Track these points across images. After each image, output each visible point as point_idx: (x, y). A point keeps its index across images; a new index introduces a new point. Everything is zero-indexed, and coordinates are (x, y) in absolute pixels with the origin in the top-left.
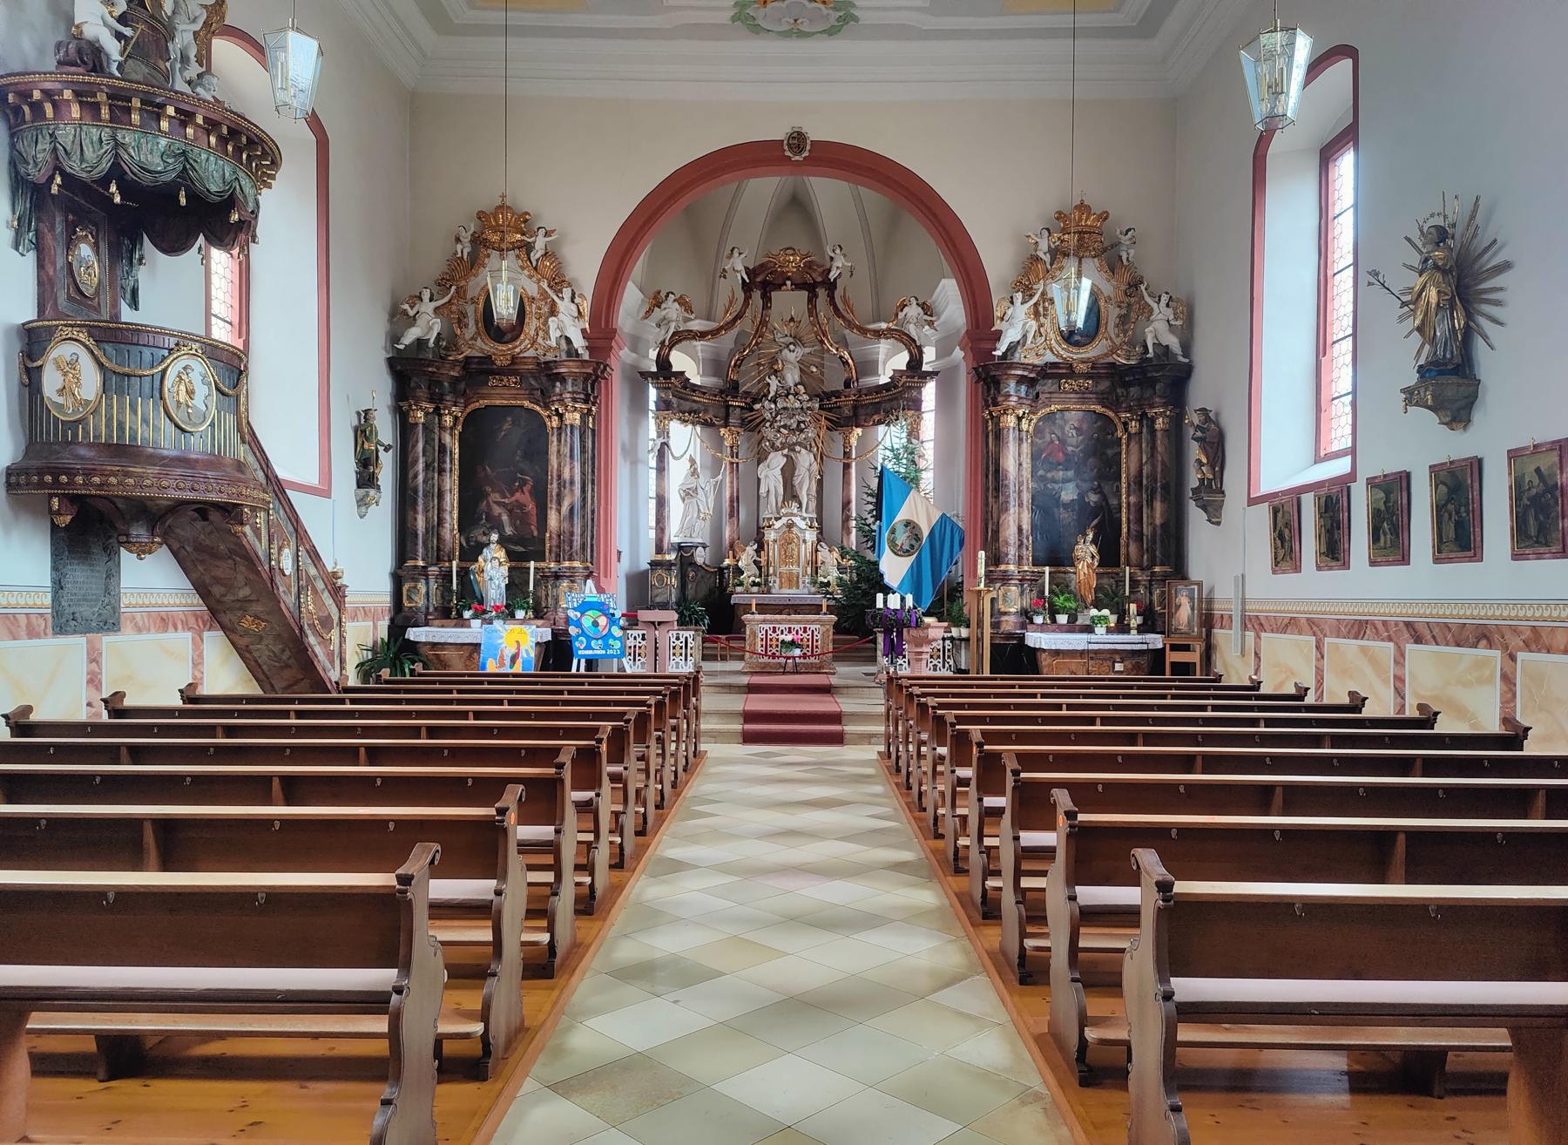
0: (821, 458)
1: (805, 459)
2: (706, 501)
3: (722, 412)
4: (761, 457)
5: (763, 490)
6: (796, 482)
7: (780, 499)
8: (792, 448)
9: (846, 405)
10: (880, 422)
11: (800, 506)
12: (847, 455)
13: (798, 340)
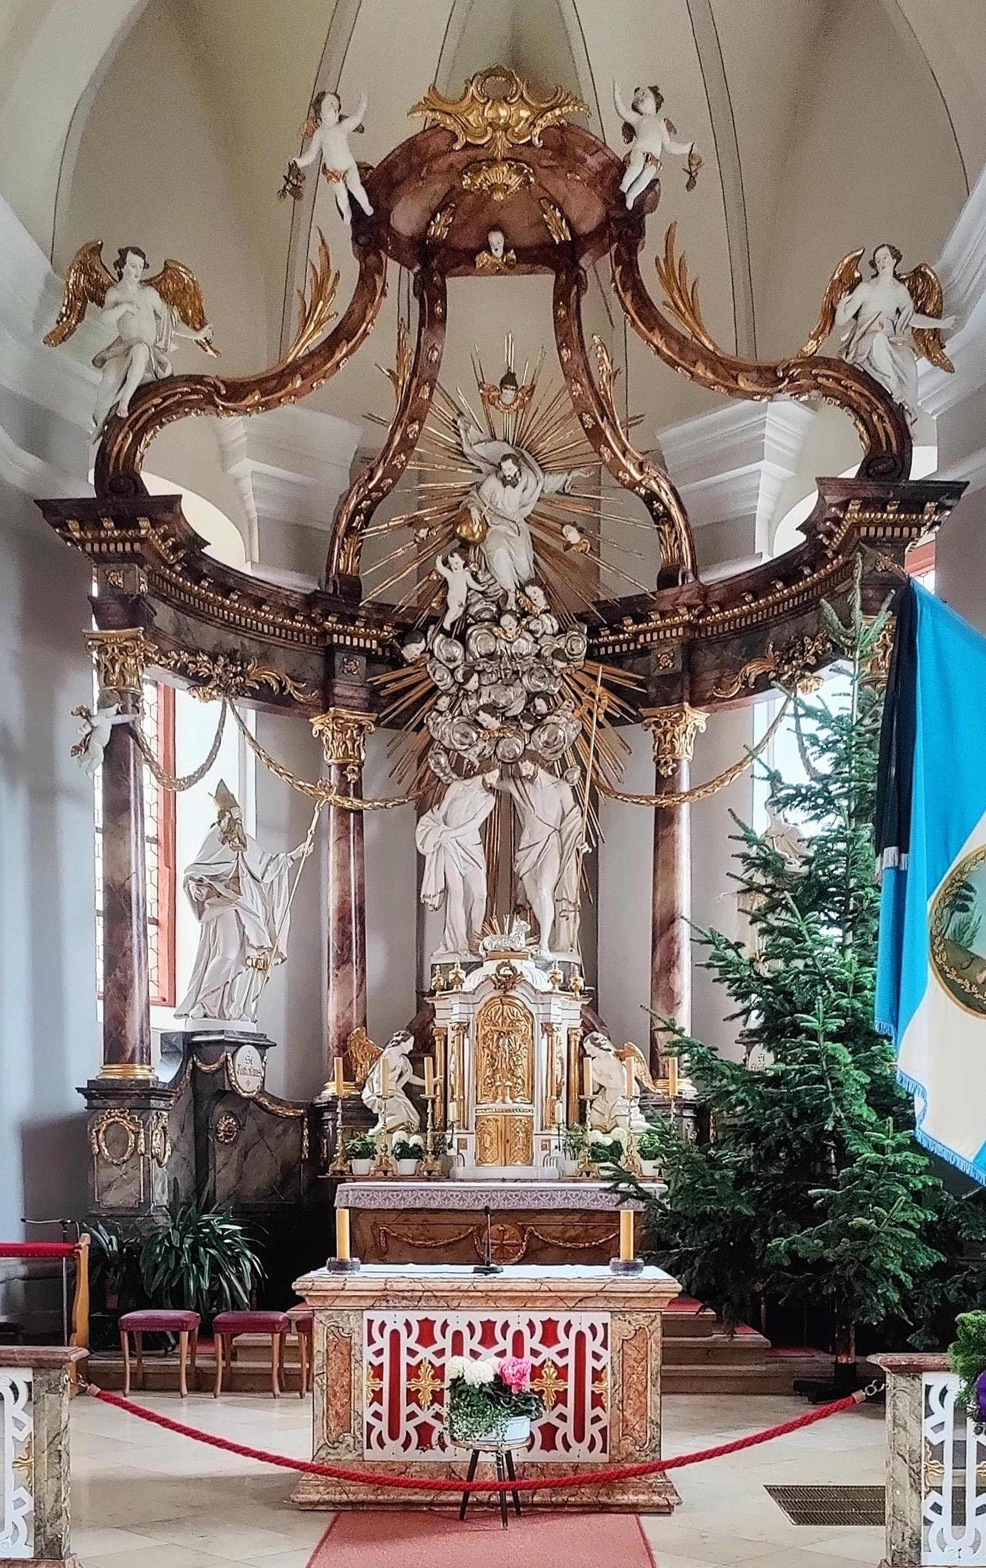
0: (593, 797)
1: (549, 801)
2: (269, 913)
3: (316, 662)
4: (426, 797)
5: (431, 886)
6: (524, 864)
7: (479, 911)
8: (510, 770)
9: (664, 636)
10: (762, 684)
11: (535, 931)
12: (665, 784)
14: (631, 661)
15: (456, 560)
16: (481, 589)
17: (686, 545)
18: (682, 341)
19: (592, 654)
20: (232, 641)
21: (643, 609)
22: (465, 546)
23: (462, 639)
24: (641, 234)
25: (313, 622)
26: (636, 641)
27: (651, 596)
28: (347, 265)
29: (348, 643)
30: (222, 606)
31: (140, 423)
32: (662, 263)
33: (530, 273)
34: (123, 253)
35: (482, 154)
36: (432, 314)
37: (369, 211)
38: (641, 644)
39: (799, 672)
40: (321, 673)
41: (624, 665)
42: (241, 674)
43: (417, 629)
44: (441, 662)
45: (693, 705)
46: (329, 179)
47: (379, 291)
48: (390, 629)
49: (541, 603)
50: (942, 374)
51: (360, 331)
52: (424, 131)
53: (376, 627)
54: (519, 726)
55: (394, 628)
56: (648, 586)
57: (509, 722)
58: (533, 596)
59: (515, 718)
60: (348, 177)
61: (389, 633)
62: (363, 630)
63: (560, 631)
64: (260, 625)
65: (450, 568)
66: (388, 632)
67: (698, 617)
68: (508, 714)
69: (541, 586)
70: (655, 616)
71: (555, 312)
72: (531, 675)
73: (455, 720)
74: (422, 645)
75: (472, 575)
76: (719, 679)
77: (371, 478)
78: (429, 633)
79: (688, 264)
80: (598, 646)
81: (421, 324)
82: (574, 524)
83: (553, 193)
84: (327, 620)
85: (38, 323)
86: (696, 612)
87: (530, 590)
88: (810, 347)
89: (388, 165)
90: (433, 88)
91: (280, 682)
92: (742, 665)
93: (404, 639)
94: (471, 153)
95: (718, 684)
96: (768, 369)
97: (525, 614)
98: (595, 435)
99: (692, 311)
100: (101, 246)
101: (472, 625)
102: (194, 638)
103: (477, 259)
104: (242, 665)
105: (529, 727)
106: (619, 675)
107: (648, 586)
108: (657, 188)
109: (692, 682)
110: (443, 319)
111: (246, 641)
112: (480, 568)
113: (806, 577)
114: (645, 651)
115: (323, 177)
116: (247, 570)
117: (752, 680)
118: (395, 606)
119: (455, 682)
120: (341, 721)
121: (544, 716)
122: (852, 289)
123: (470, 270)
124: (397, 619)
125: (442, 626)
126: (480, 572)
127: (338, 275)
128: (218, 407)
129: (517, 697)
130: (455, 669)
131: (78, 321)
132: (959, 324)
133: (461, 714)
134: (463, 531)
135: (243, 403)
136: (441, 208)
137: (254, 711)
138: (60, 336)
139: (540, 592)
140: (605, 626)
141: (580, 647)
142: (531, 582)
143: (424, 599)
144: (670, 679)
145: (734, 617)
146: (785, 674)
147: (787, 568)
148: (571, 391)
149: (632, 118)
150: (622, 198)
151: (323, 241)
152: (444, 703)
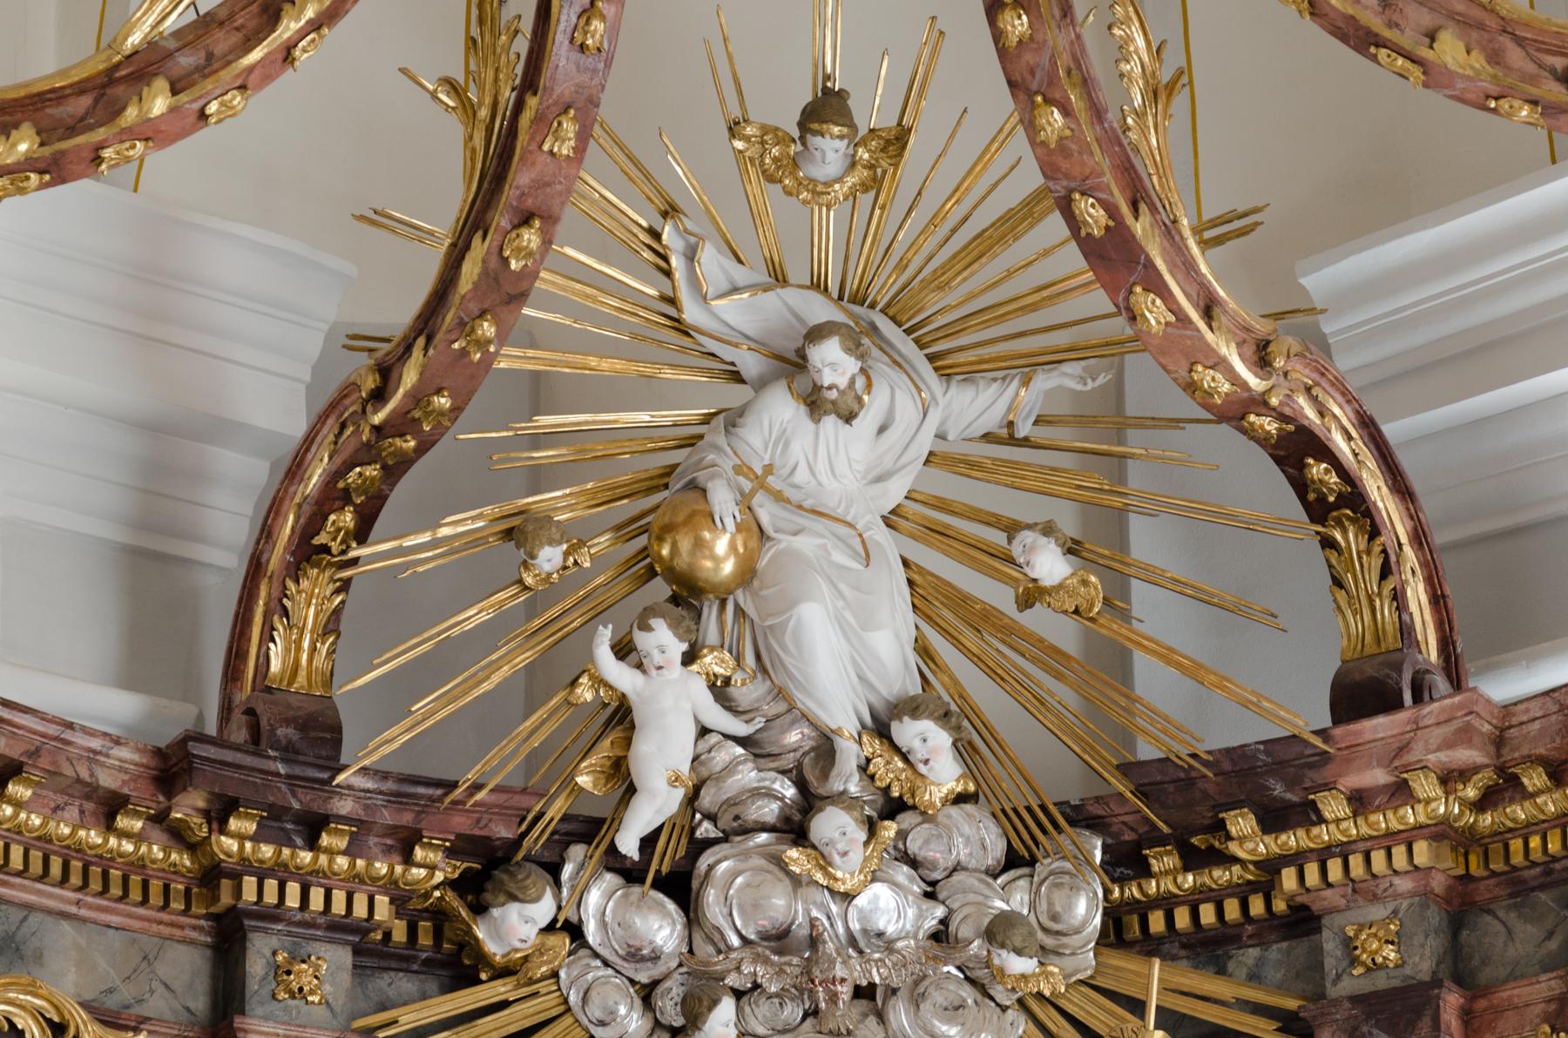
3: (183, 970)
14: (1253, 953)
15: (663, 641)
16: (741, 728)
17: (1417, 594)
19: (1118, 930)
21: (1291, 784)
22: (688, 596)
25: (178, 835)
26: (1267, 888)
27: (1317, 741)
29: (293, 901)
38: (1290, 899)
40: (200, 1003)
41: (1231, 966)
43: (527, 858)
44: (606, 964)
49: (944, 773)
53: (388, 850)
55: (451, 853)
58: (919, 752)
61: (432, 868)
62: (342, 862)
63: (1012, 860)
65: (639, 666)
66: (431, 869)
67: (1480, 805)
69: (944, 718)
70: (1333, 806)
72: (916, 1001)
74: (544, 910)
75: (712, 687)
77: (379, 396)
78: (567, 871)
80: (1142, 909)
82: (1048, 530)
84: (223, 831)
86: (1471, 793)
87: (908, 732)
93: (479, 890)
97: (893, 807)
98: (1114, 257)
101: (709, 843)
107: (1309, 712)
109: (1467, 1015)
112: (738, 659)
114: (1302, 921)
118: (454, 785)
119: (657, 1024)
124: (461, 823)
125: (612, 850)
126: (738, 678)
130: (655, 983)
139: (940, 739)
140: (1162, 841)
141: (1084, 911)
142: (910, 707)
143: (552, 766)
148: (1031, 127)
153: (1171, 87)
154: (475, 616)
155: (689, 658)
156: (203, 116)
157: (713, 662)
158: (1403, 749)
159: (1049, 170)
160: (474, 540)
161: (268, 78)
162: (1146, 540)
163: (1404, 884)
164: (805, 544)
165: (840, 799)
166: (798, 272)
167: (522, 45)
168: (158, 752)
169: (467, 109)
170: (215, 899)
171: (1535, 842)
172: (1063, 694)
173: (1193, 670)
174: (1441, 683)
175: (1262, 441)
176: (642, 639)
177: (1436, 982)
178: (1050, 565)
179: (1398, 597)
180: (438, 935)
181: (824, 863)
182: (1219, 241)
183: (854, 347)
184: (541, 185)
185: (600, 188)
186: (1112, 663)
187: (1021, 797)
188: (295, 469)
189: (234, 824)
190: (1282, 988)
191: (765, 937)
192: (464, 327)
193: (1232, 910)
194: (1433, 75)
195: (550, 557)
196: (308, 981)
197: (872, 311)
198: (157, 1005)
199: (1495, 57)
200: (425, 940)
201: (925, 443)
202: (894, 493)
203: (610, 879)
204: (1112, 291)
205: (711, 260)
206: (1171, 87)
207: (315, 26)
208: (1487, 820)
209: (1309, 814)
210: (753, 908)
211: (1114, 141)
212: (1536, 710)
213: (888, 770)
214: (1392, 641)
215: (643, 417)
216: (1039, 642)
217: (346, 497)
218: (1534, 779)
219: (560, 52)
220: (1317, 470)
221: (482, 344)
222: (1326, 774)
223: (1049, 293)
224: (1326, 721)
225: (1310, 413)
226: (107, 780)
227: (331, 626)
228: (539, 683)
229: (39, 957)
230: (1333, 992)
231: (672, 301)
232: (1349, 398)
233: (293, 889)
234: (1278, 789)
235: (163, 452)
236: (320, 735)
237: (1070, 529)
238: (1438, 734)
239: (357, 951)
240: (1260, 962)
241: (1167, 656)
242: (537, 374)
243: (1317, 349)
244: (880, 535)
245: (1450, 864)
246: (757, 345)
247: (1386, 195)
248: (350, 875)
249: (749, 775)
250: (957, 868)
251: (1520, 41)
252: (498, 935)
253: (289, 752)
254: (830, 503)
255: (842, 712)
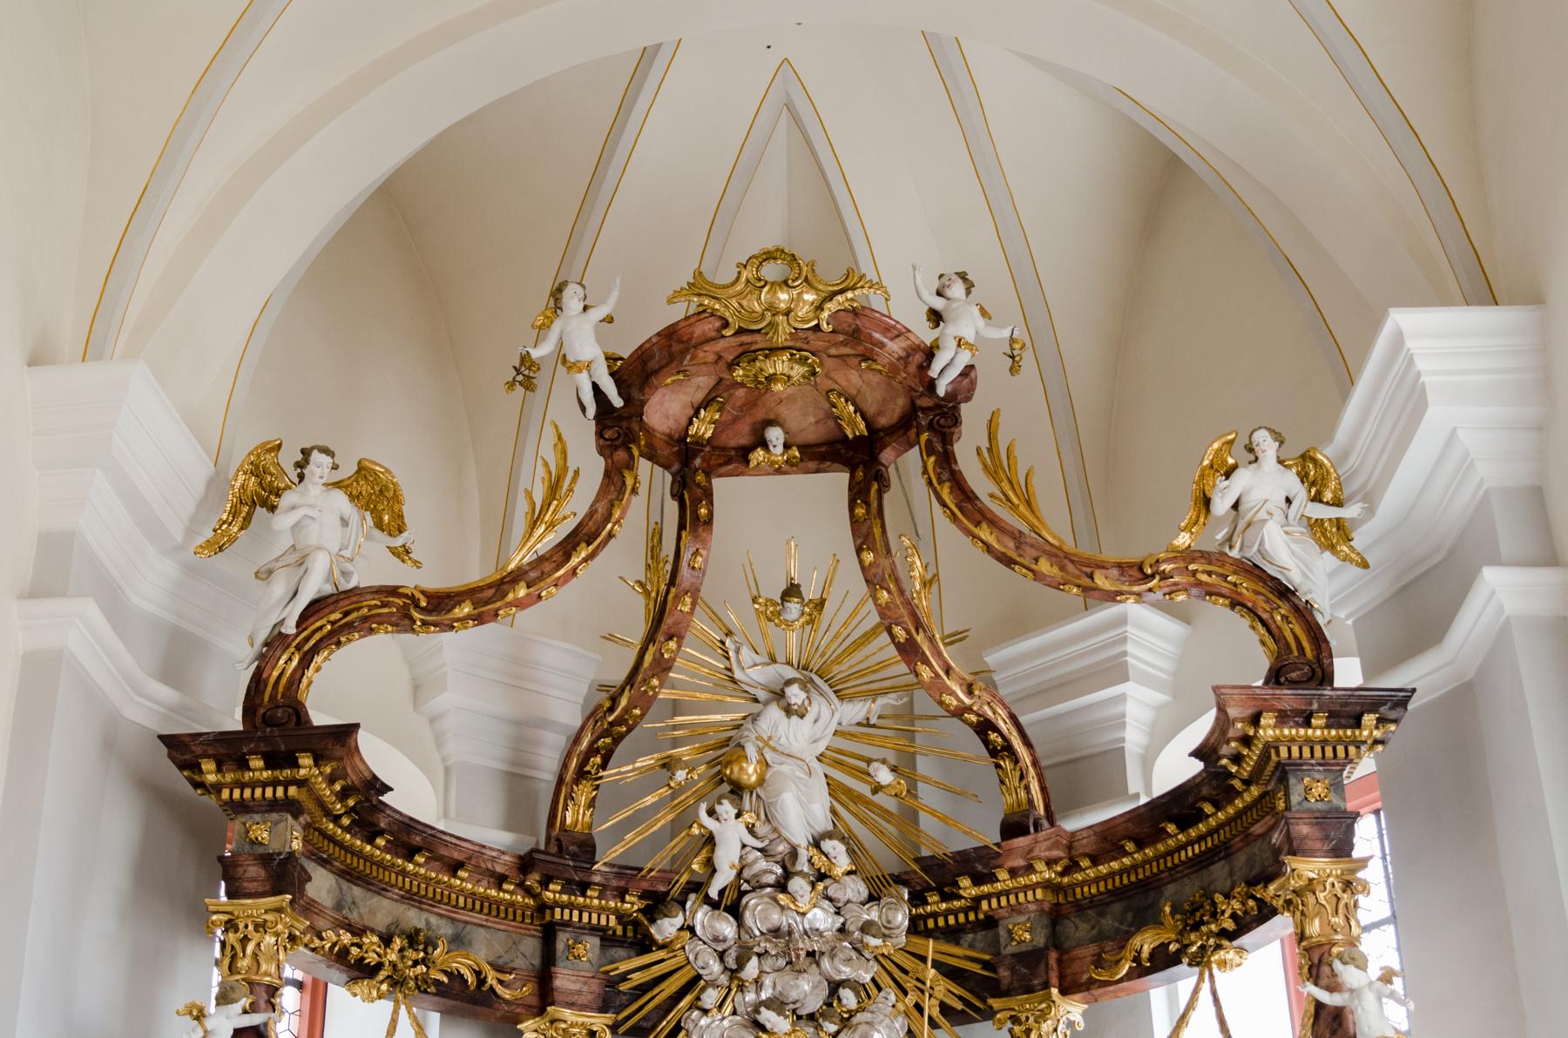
3: (530, 947)
9: (1020, 897)
10: (1163, 960)
13: (817, 674)
15: (727, 809)
16: (759, 845)
18: (1018, 537)
19: (916, 927)
20: (414, 918)
22: (738, 790)
23: (735, 911)
24: (957, 421)
25: (528, 892)
28: (589, 465)
29: (576, 919)
30: (404, 873)
31: (312, 642)
32: (986, 455)
33: (817, 471)
34: (306, 453)
35: (760, 341)
36: (694, 513)
37: (618, 402)
38: (985, 913)
39: (1212, 941)
40: (537, 962)
42: (424, 961)
45: (1064, 992)
46: (569, 368)
47: (629, 488)
48: (634, 899)
49: (843, 862)
50: (1354, 571)
51: (604, 533)
52: (687, 318)
53: (614, 897)
54: (819, 1027)
55: (641, 898)
56: (990, 836)
57: (802, 1022)
58: (832, 853)
59: (811, 1017)
60: (593, 367)
62: (596, 902)
63: (872, 898)
64: (454, 896)
66: (632, 904)
68: (803, 1012)
69: (842, 839)
70: (1002, 875)
71: (851, 510)
72: (832, 957)
73: (726, 1023)
74: (679, 921)
76: (1099, 955)
77: (611, 710)
79: (1017, 452)
80: (925, 918)
81: (682, 526)
82: (884, 762)
83: (844, 383)
85: (190, 532)
86: (1059, 869)
87: (827, 845)
88: (1183, 540)
89: (642, 355)
90: (699, 274)
91: (478, 973)
92: (1128, 936)
94: (745, 338)
95: (1098, 963)
96: (1131, 565)
97: (822, 877)
98: (909, 651)
99: (1028, 503)
100: (280, 446)
101: (747, 892)
102: (360, 915)
103: (751, 456)
104: (425, 950)
105: (832, 1028)
106: (957, 954)
107: (991, 836)
108: (973, 375)
109: (1060, 962)
110: (709, 521)
111: (434, 920)
113: (1208, 816)
114: (990, 923)
115: (561, 369)
116: (441, 826)
117: (1145, 954)
119: (726, 968)
120: (563, 1026)
121: (852, 1013)
122: (1228, 475)
123: (742, 468)
124: (645, 885)
125: (707, 895)
127: (577, 473)
128: (414, 622)
129: (814, 988)
130: (725, 951)
131: (242, 529)
132: (1370, 511)
133: (734, 1013)
134: (733, 771)
135: (450, 616)
136: (706, 403)
137: (438, 1015)
138: (217, 546)
140: (932, 889)
141: (901, 918)
142: (829, 835)
144: (1031, 959)
145: (1112, 874)
146: (1192, 944)
147: (1179, 806)
148: (875, 599)
149: (938, 304)
150: (931, 385)
151: (560, 438)
152: (710, 997)
153: (931, 582)
154: (650, 800)
155: (738, 816)
156: (540, 597)
157: (748, 817)
158: (1031, 851)
159: (882, 615)
160: (650, 768)
161: (566, 582)
162: (924, 766)
163: (1032, 907)
164: (785, 768)
165: (800, 873)
166: (781, 658)
167: (669, 567)
168: (520, 857)
169: (647, 593)
170: (543, 918)
171: (1086, 889)
172: (891, 829)
173: (944, 819)
174: (1045, 823)
175: (971, 724)
176: (718, 808)
177: (1046, 948)
178: (884, 776)
179: (1027, 788)
180: (635, 932)
181: (794, 900)
182: (951, 643)
183: (804, 688)
184: (677, 623)
185: (700, 624)
186: (910, 816)
187: (875, 872)
188: (577, 740)
189: (551, 887)
190: (983, 951)
191: (770, 931)
192: (645, 681)
193: (962, 918)
194: (1038, 577)
195: (681, 775)
196: (582, 952)
197: (811, 674)
198: (519, 963)
199: (1062, 568)
200: (630, 934)
201: (833, 727)
202: (821, 747)
203: (706, 907)
204: (908, 664)
205: (746, 653)
206: (931, 582)
207: (585, 560)
208: (1066, 880)
209: (993, 879)
210: (765, 919)
211: (908, 603)
212: (1085, 834)
213: (820, 861)
214: (1025, 806)
215: (718, 717)
216: (881, 808)
217: (597, 751)
218: (1085, 863)
219: (684, 571)
220: (993, 736)
221: (653, 688)
222: (1000, 861)
223: (883, 665)
224: (998, 840)
225: (990, 713)
226: (499, 869)
227: (591, 804)
228: (676, 827)
229: (470, 944)
230: (1004, 952)
231: (730, 670)
232: (1005, 707)
233: (576, 913)
234: (980, 868)
235: (523, 731)
236: (586, 848)
237: (892, 761)
238: (1044, 845)
239: (602, 939)
240: (974, 940)
241: (933, 813)
242: (675, 701)
243: (991, 687)
244: (815, 764)
245: (1050, 897)
246: (765, 687)
247: (1017, 624)
248: (598, 908)
249: (763, 864)
250: (849, 901)
251: (1072, 562)
252: (660, 932)
253: (574, 857)
254: (795, 751)
255: (801, 838)
